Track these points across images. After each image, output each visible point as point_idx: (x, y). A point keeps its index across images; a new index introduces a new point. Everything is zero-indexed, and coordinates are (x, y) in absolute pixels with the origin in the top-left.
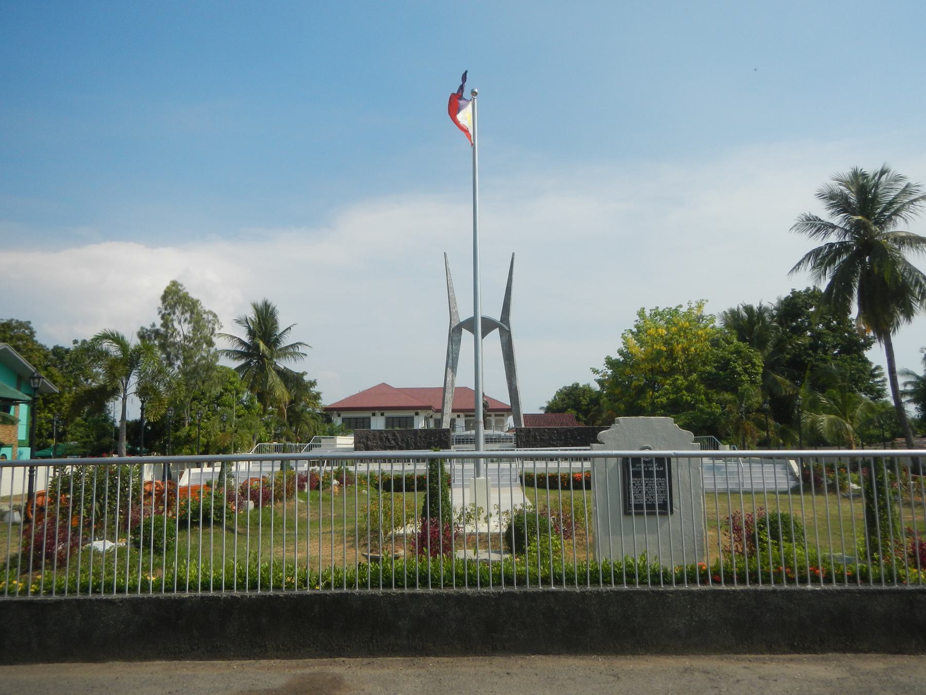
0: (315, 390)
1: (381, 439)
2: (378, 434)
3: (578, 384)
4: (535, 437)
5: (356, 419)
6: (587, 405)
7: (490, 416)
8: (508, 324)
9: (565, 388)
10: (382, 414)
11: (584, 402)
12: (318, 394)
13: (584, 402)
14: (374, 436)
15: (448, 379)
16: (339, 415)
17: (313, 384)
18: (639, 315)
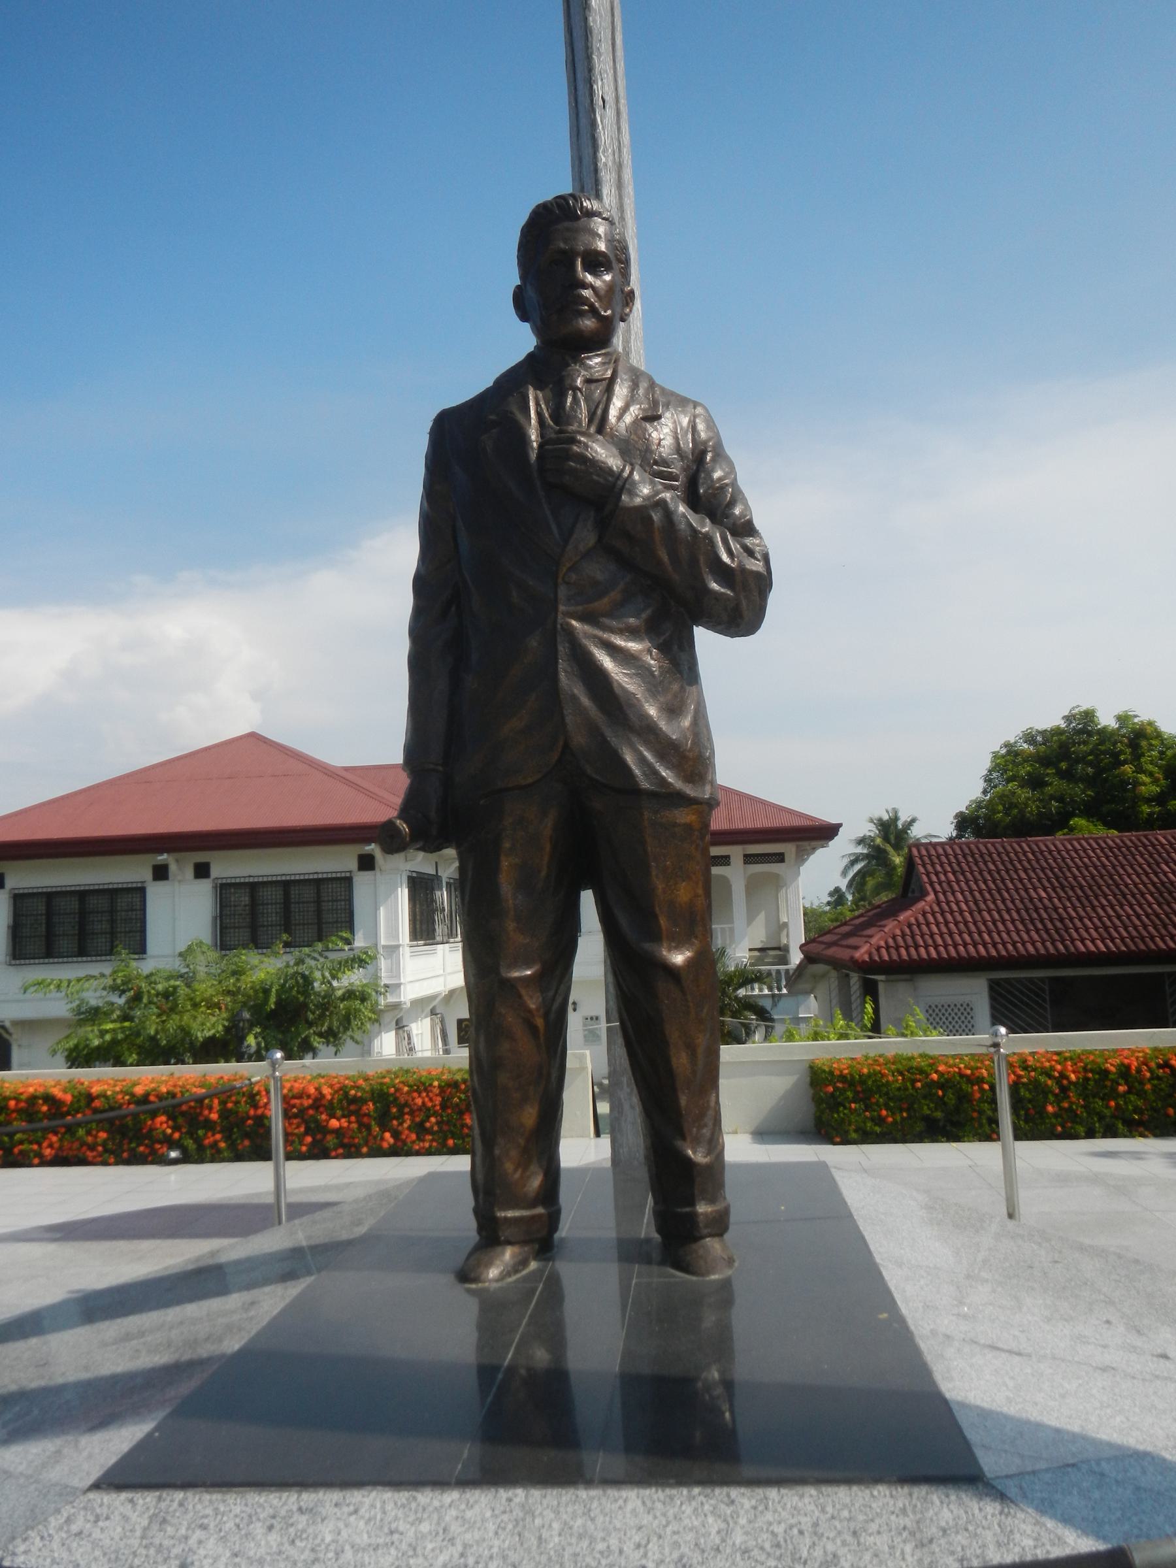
3: (1088, 716)
5: (83, 895)
6: (1160, 799)
7: (724, 860)
9: (1030, 738)
10: (202, 871)
11: (1148, 787)
13: (1148, 787)
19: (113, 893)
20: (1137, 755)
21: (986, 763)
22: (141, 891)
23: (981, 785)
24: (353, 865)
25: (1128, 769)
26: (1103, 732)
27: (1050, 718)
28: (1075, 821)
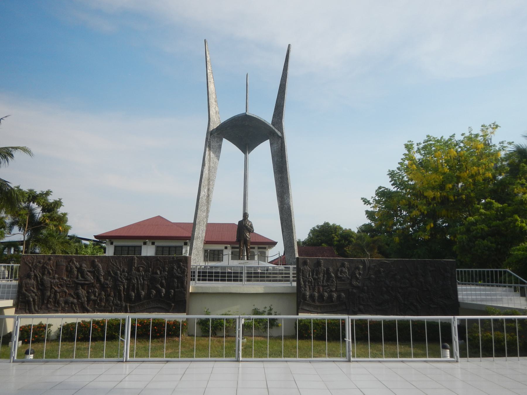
0: (61, 211)
1: (69, 272)
2: (64, 264)
4: (327, 272)
5: (128, 247)
6: (339, 241)
7: (254, 248)
8: (281, 129)
9: (318, 226)
10: (153, 244)
12: (65, 215)
13: (336, 238)
14: (57, 265)
15: (202, 193)
16: (112, 243)
17: (58, 204)
18: (407, 146)
19: (135, 247)
20: (336, 232)
21: (309, 231)
22: (141, 247)
23: (308, 236)
24: (183, 244)
25: (333, 235)
26: (331, 226)
27: (321, 223)
28: (323, 244)
